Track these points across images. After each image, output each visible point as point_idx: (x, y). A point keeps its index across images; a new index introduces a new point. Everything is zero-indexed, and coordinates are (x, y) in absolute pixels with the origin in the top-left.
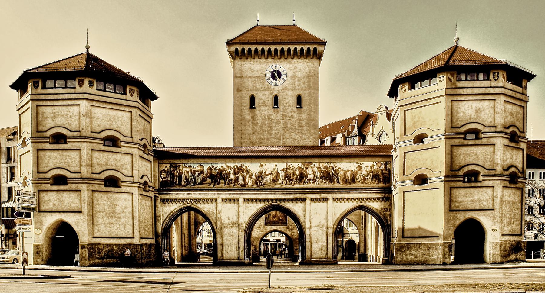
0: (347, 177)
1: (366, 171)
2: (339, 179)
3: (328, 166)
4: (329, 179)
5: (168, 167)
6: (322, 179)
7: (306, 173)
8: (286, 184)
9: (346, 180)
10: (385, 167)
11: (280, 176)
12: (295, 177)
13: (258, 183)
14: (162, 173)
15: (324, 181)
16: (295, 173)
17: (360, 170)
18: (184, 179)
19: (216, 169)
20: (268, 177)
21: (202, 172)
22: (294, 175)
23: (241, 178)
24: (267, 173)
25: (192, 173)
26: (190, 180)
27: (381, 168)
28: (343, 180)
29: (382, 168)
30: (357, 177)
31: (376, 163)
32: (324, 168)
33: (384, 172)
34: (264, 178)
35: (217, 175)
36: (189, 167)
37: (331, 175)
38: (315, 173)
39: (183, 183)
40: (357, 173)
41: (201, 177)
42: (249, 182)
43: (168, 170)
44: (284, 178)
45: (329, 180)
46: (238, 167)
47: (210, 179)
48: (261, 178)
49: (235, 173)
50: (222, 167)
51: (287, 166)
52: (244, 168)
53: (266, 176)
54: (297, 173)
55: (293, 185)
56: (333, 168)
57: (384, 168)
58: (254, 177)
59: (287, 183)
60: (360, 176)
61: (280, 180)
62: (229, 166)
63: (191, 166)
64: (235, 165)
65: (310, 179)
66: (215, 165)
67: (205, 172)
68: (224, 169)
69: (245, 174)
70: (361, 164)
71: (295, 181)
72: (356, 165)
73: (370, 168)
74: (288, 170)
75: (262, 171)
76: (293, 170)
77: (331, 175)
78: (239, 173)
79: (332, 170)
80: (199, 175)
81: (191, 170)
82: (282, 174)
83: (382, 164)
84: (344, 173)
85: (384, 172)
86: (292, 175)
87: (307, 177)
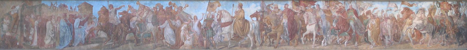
0: (384, 31)
1: (421, 19)
2: (369, 35)
3: (346, 9)
4: (349, 34)
5: (18, 7)
6: (336, 35)
7: (303, 21)
8: (261, 45)
9: (384, 37)
10: (457, 12)
11: (249, 27)
12: (280, 29)
13: (205, 42)
14: (5, 20)
15: (339, 39)
16: (281, 22)
17: (408, 17)
18: (49, 32)
19: (118, 11)
20: (226, 29)
21: (89, 19)
22: (278, 23)
23: (169, 32)
24: (223, 21)
25: (66, 21)
26: (62, 34)
27: (449, 14)
28: (376, 38)
29: (451, 13)
30: (404, 30)
31: (440, 4)
32: (337, 12)
33: (455, 22)
34: (217, 32)
35: (119, 24)
36: (60, 6)
37: (353, 26)
38: (320, 23)
39: (47, 41)
40: (403, 23)
41: (87, 28)
42: (185, 39)
43: (17, 13)
44: (257, 32)
45: (348, 37)
46: (164, 8)
47: (105, 31)
48: (210, 32)
49: (156, 22)
50: (130, 7)
51: (263, 7)
52: (176, 10)
53: (222, 27)
54: (285, 21)
55: (276, 47)
56: (356, 13)
57: (454, 13)
58: (195, 28)
59: (263, 42)
60: (411, 29)
61: (249, 35)
62: (144, 6)
63: (65, 6)
64: (158, 5)
65: (311, 35)
66: (116, 4)
67: (95, 18)
68: (135, 11)
69: (178, 22)
70: (411, 6)
71: (280, 38)
72: (401, 7)
73: (427, 14)
74: (266, 16)
75: (213, 17)
76: (276, 15)
77: (353, 26)
78: (166, 22)
79: (354, 16)
80: (82, 24)
81: (65, 15)
82: (254, 23)
83: (451, 5)
84: (379, 23)
85: (455, 21)
86: (273, 26)
87: (305, 30)
